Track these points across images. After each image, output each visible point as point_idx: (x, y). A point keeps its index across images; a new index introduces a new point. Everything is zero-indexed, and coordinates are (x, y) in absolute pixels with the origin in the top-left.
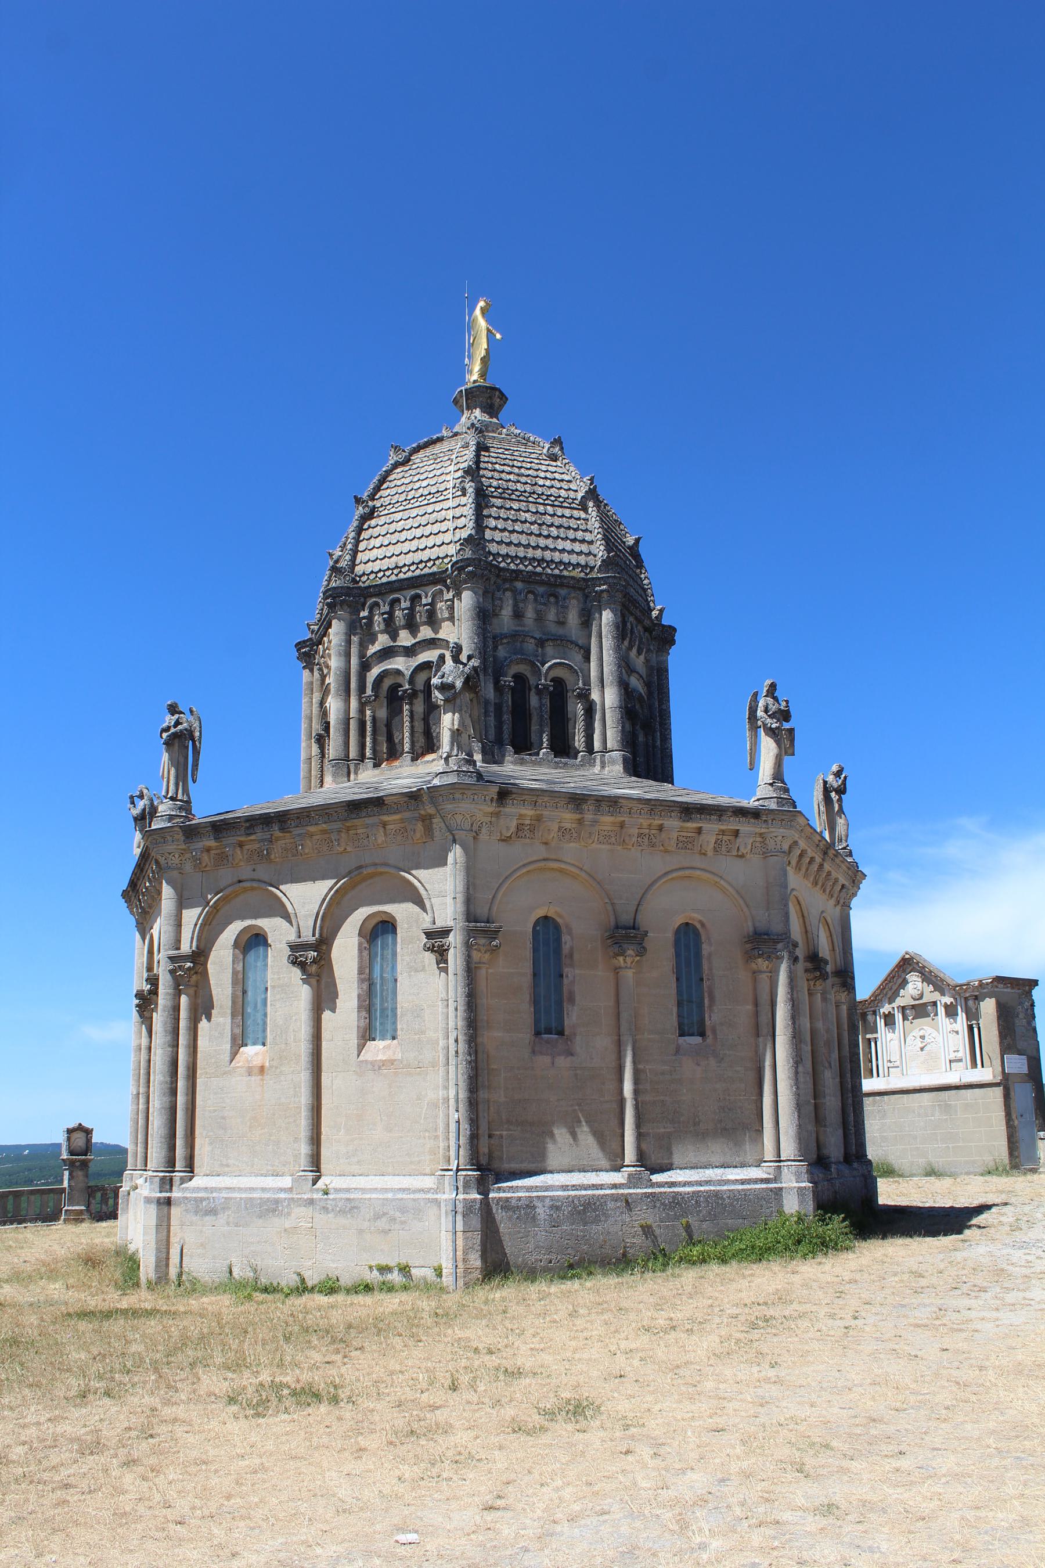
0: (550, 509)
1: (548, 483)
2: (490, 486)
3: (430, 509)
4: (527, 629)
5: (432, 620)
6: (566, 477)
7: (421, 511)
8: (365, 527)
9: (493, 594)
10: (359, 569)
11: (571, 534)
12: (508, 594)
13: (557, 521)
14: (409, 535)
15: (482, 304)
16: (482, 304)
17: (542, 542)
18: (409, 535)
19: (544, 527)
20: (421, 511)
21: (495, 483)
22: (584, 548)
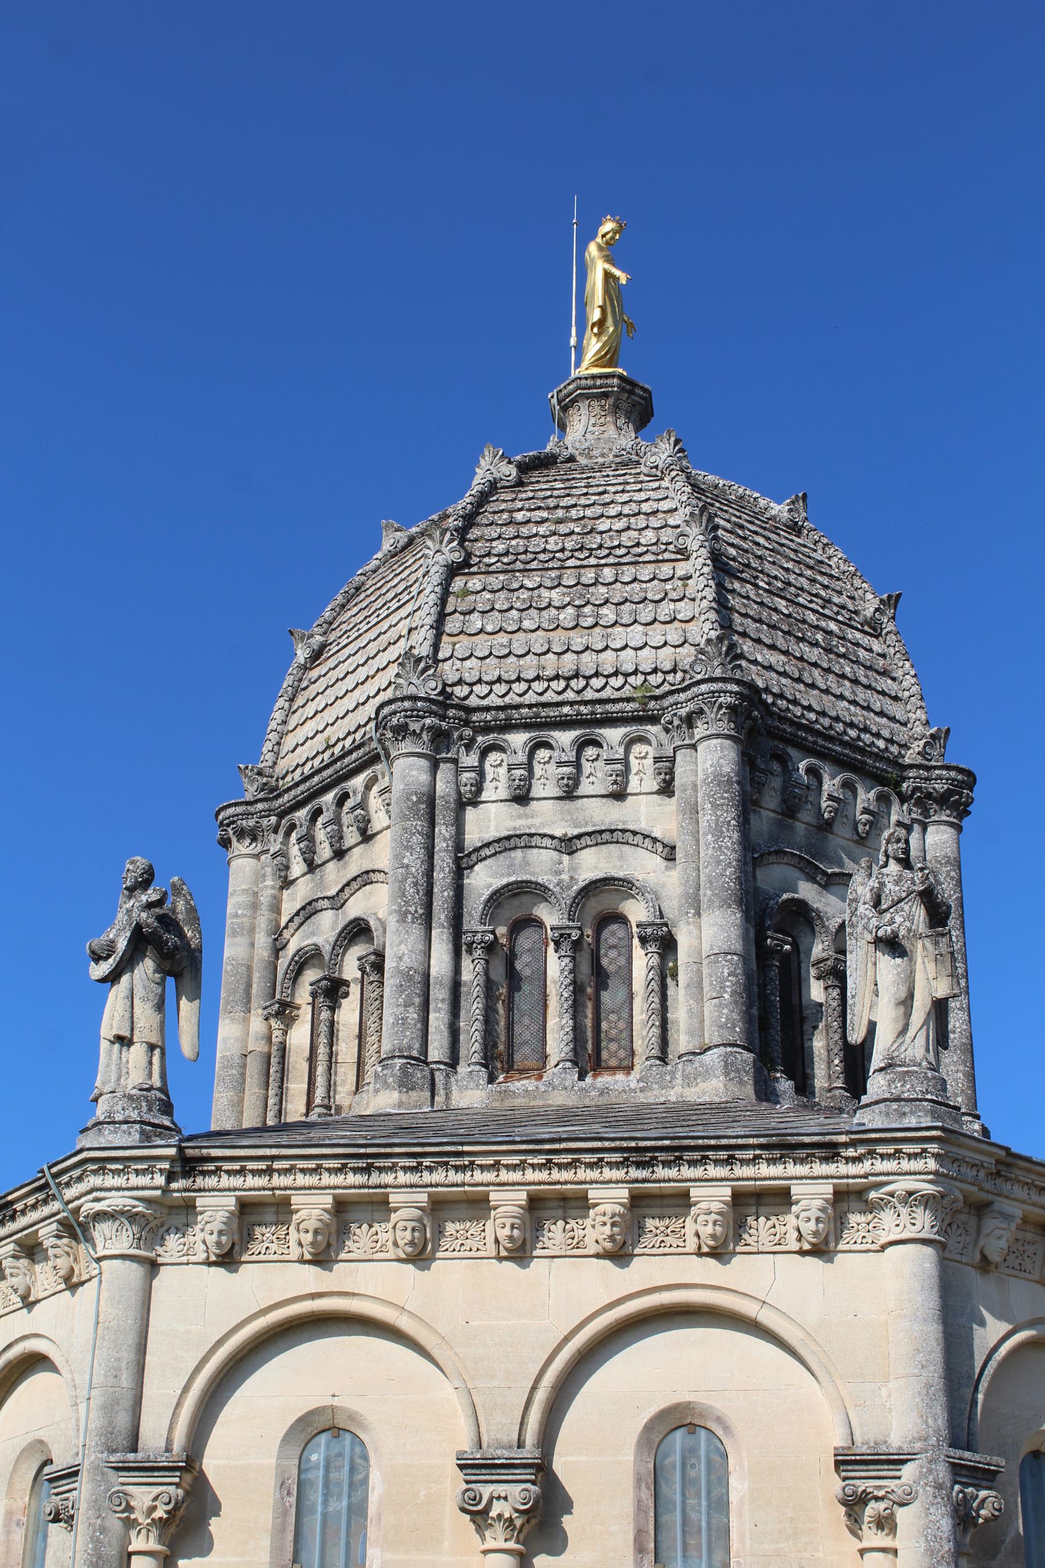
0: (608, 574)
1: (619, 525)
2: (489, 555)
3: (385, 625)
4: (537, 821)
5: (367, 837)
6: (665, 505)
7: (372, 635)
8: (304, 684)
9: (455, 761)
10: (283, 766)
11: (646, 613)
12: (494, 757)
13: (618, 593)
14: (350, 682)
15: (608, 226)
16: (608, 226)
17: (578, 641)
18: (350, 682)
19: (587, 610)
20: (372, 635)
21: (500, 547)
22: (673, 634)
